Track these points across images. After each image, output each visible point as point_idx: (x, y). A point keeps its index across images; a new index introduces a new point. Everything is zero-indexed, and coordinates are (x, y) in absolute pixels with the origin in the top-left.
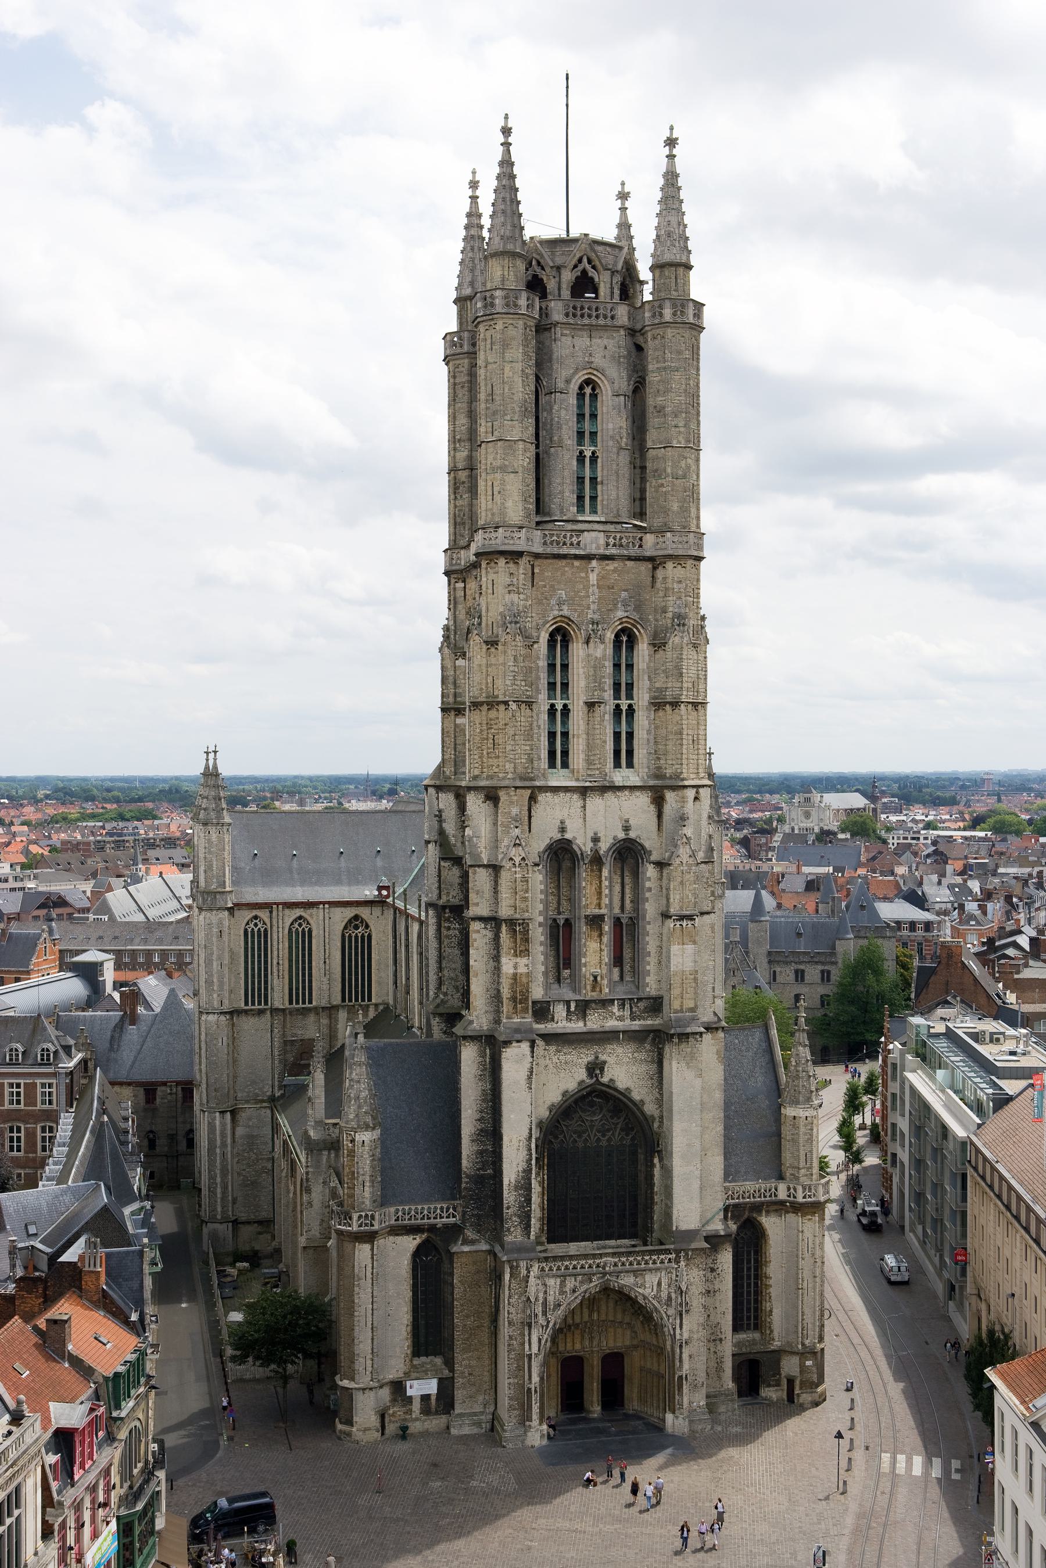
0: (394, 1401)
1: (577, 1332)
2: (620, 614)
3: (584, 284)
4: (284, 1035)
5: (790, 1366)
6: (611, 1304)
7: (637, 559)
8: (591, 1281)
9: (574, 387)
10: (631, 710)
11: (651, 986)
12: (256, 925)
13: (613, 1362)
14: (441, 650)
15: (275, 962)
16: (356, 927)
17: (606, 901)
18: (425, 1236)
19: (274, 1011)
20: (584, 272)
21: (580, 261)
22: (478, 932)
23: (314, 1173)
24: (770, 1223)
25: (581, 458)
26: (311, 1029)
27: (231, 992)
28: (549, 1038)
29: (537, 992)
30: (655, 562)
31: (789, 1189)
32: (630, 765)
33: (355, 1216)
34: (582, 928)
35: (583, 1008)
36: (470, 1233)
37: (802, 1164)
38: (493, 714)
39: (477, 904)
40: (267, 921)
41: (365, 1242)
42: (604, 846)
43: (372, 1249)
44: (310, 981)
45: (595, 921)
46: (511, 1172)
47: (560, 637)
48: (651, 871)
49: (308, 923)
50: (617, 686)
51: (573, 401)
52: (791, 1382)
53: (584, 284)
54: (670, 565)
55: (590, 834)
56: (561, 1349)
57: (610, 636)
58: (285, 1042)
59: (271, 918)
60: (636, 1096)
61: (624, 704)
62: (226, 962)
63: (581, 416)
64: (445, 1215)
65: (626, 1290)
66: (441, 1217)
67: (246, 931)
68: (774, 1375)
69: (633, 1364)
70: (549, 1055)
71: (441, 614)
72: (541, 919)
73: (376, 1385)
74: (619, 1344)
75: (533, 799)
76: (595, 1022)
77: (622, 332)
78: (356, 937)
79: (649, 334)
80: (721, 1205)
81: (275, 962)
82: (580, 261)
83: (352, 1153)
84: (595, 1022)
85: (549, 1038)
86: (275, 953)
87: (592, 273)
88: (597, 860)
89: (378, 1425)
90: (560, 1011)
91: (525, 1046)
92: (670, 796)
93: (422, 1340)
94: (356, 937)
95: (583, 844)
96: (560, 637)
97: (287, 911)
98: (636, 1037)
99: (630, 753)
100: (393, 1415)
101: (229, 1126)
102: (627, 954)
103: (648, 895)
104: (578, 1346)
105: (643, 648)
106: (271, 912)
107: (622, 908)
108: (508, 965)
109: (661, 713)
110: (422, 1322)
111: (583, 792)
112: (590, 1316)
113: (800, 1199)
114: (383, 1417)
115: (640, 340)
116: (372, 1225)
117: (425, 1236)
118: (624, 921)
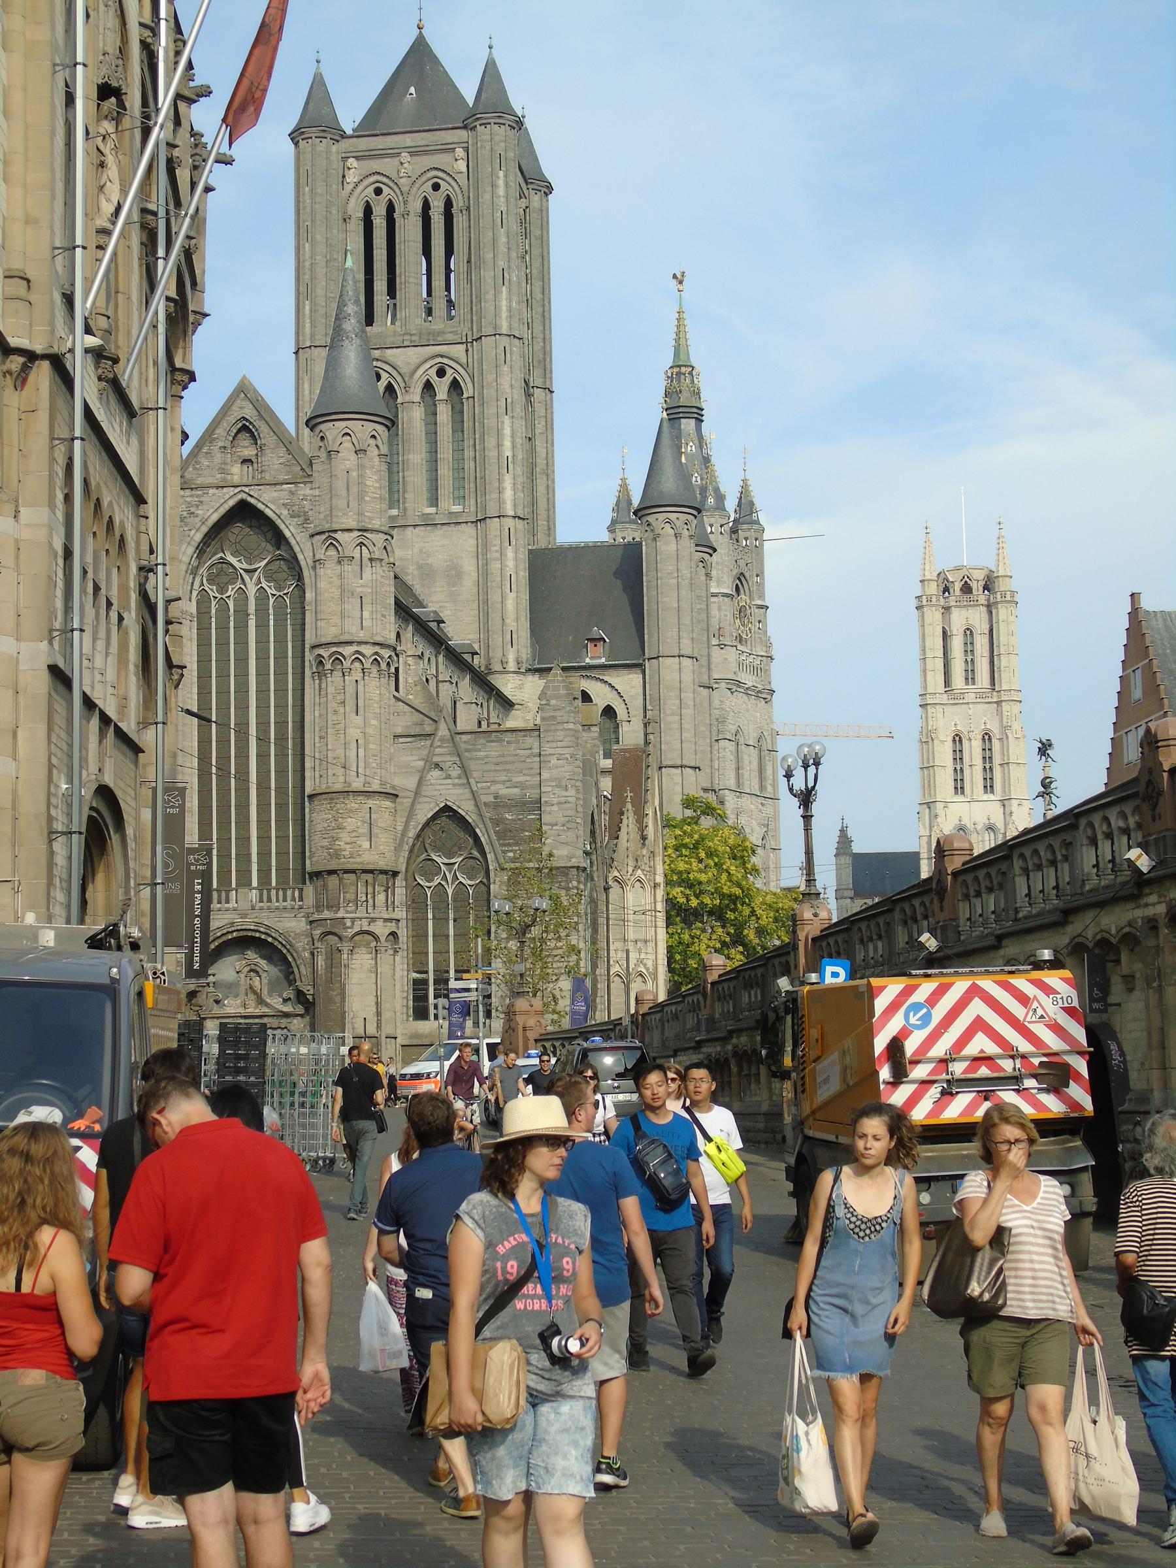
3: (967, 589)
42: (979, 827)
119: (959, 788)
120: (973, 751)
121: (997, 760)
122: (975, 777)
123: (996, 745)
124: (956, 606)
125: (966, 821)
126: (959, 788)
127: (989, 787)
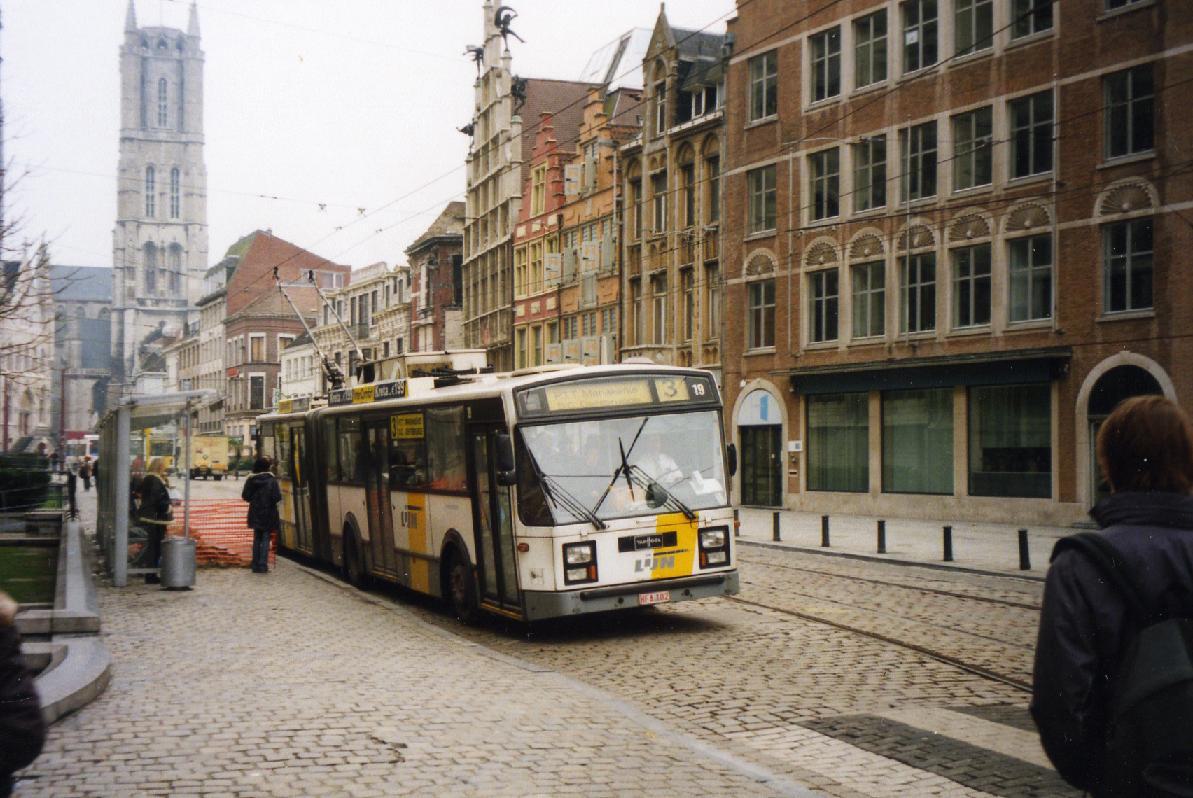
7: (180, 142)
10: (177, 198)
11: (183, 298)
28: (145, 312)
29: (139, 294)
30: (186, 144)
32: (177, 216)
34: (157, 274)
35: (157, 302)
36: (114, 379)
42: (166, 245)
45: (163, 271)
46: (127, 354)
47: (151, 169)
48: (184, 255)
51: (155, 86)
53: (162, 43)
54: (190, 145)
57: (169, 169)
61: (175, 195)
70: (144, 318)
75: (138, 226)
76: (162, 307)
84: (162, 307)
85: (145, 312)
88: (163, 249)
90: (149, 302)
91: (132, 311)
92: (189, 227)
95: (158, 244)
96: (151, 169)
98: (178, 313)
99: (177, 213)
102: (175, 285)
105: (182, 177)
119: (150, 211)
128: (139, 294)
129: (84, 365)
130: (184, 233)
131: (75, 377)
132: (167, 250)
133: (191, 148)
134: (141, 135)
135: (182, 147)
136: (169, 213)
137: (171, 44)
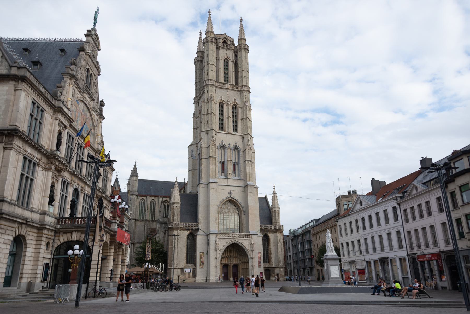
0: (181, 274)
1: (227, 258)
2: (234, 101)
3: (225, 42)
4: (148, 227)
5: (277, 271)
6: (235, 252)
8: (231, 240)
9: (223, 59)
12: (142, 201)
13: (235, 266)
14: (193, 117)
15: (147, 209)
16: (166, 203)
17: (232, 158)
18: (190, 231)
19: (146, 220)
20: (225, 41)
21: (224, 38)
22: (204, 161)
23: (160, 229)
24: (271, 235)
25: (225, 73)
26: (154, 225)
27: (136, 215)
31: (274, 227)
33: (174, 223)
37: (277, 221)
38: (208, 116)
39: (204, 155)
40: (145, 200)
41: (176, 230)
42: (232, 146)
43: (178, 232)
44: (155, 215)
47: (221, 105)
48: (241, 153)
49: (155, 201)
50: (233, 116)
52: (277, 275)
54: (244, 92)
55: (228, 144)
56: (223, 262)
57: (232, 105)
58: (148, 228)
59: (146, 199)
60: (239, 201)
62: (135, 208)
63: (225, 65)
64: (195, 226)
65: (239, 244)
66: (194, 227)
67: (140, 202)
68: (273, 274)
69: (240, 267)
71: (193, 111)
72: (218, 160)
73: (177, 267)
74: (237, 262)
77: (233, 50)
78: (166, 205)
79: (238, 51)
80: (259, 229)
81: (147, 209)
82: (224, 38)
83: (173, 209)
86: (147, 207)
87: (226, 41)
89: (178, 279)
93: (188, 259)
94: (166, 205)
97: (150, 198)
100: (181, 278)
101: (133, 248)
103: (241, 158)
104: (227, 262)
106: (146, 198)
107: (235, 161)
108: (211, 167)
109: (242, 121)
110: (189, 255)
111: (227, 134)
112: (230, 254)
113: (277, 229)
114: (179, 276)
115: (236, 53)
116: (178, 226)
117: (190, 231)
118: (236, 163)
119: (221, 127)
120: (228, 111)
121: (240, 117)
122: (228, 124)
123: (239, 110)
124: (222, 48)
125: (225, 142)
126: (221, 127)
127: (235, 129)
128: (217, 176)
129: (181, 220)
130: (242, 140)
131: (177, 229)
132: (232, 149)
133: (245, 93)
134: (217, 85)
135: (239, 93)
136: (232, 130)
137: (229, 43)
